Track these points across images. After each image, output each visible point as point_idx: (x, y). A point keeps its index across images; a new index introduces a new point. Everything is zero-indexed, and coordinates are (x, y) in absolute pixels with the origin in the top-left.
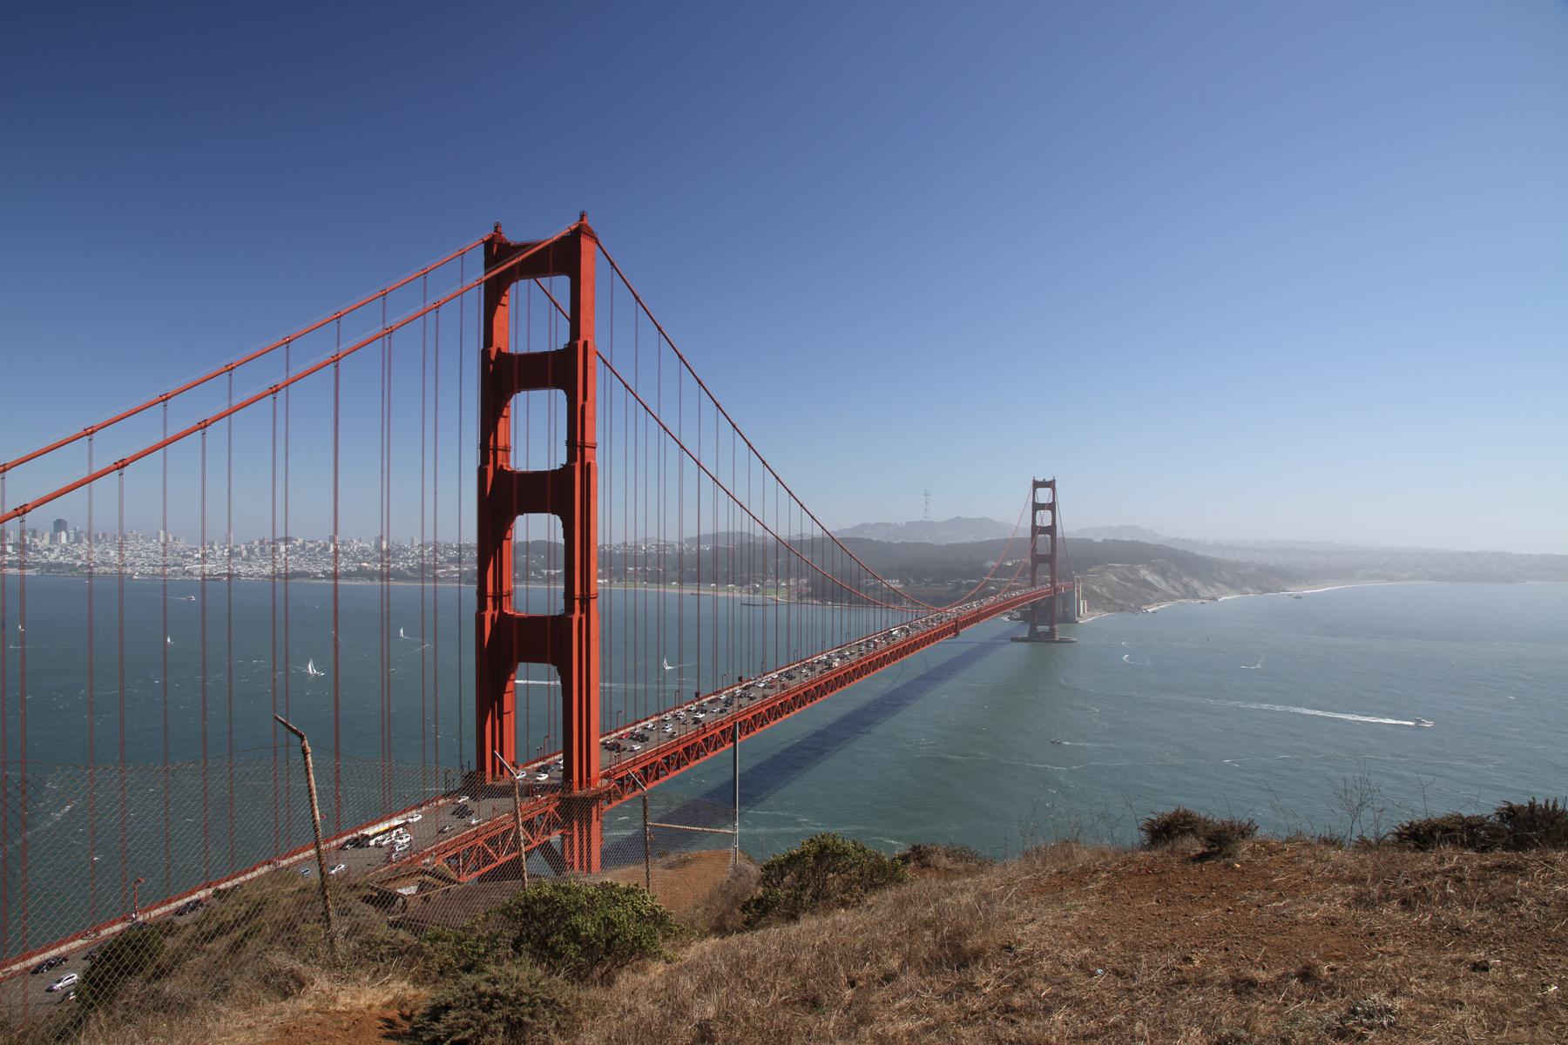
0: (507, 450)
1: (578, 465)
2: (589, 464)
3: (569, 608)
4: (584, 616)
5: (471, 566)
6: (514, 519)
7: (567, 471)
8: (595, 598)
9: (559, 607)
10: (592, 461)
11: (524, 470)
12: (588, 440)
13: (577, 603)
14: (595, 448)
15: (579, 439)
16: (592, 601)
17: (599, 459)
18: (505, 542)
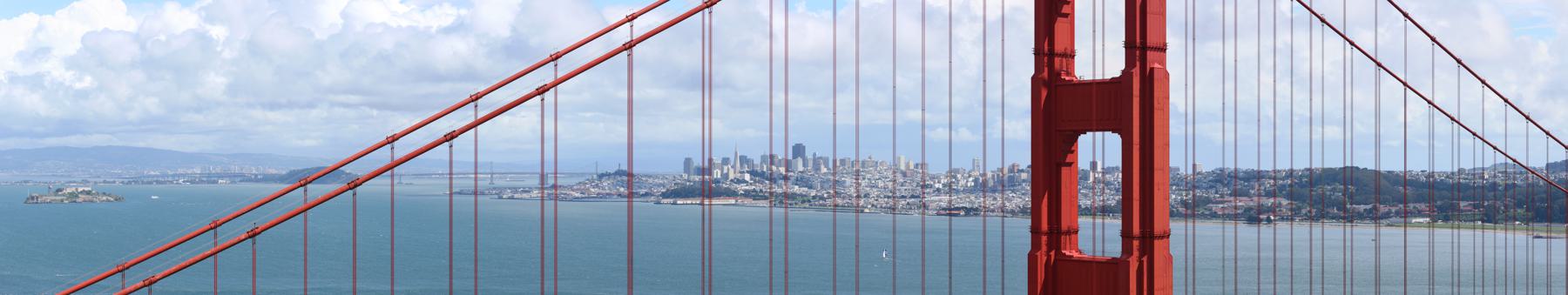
0: (1070, 55)
1: (1136, 71)
2: (1152, 69)
3: (1127, 249)
4: (1145, 259)
5: (1021, 198)
6: (1073, 140)
7: (1123, 81)
8: (1163, 237)
9: (1114, 249)
10: (1156, 65)
11: (1088, 77)
12: (1152, 40)
13: (1136, 243)
14: (1163, 49)
15: (1138, 40)
16: (1156, 242)
17: (1175, 62)
18: (1064, 170)
